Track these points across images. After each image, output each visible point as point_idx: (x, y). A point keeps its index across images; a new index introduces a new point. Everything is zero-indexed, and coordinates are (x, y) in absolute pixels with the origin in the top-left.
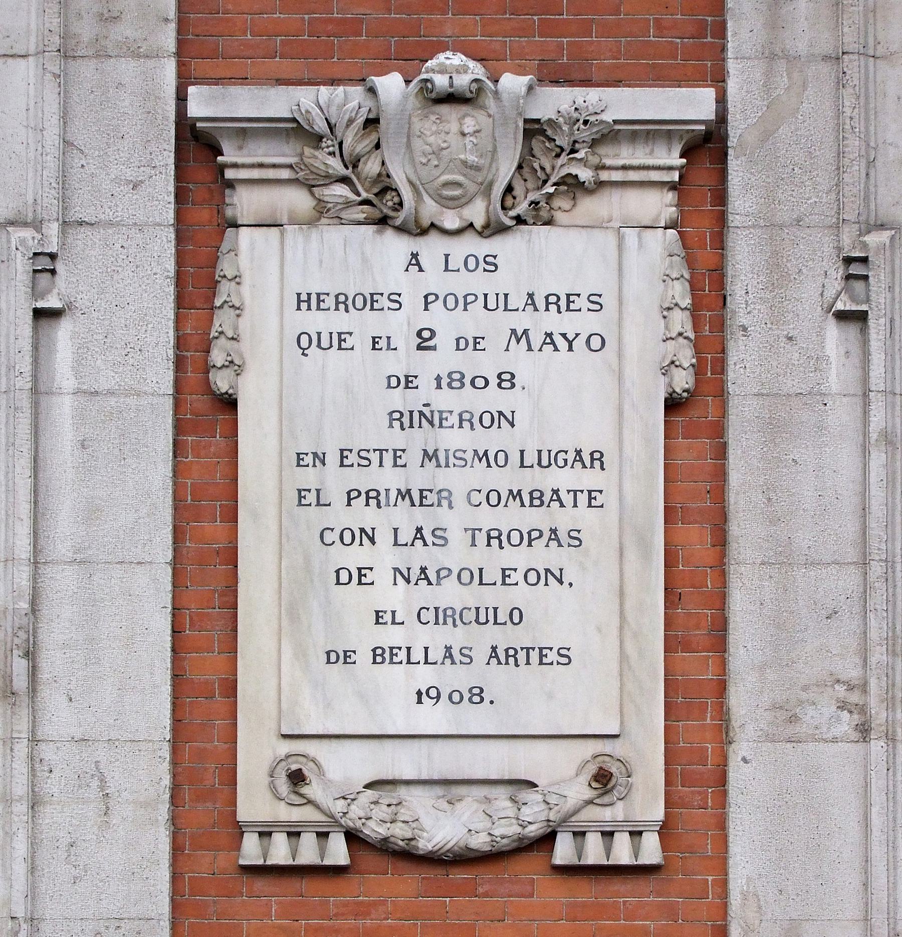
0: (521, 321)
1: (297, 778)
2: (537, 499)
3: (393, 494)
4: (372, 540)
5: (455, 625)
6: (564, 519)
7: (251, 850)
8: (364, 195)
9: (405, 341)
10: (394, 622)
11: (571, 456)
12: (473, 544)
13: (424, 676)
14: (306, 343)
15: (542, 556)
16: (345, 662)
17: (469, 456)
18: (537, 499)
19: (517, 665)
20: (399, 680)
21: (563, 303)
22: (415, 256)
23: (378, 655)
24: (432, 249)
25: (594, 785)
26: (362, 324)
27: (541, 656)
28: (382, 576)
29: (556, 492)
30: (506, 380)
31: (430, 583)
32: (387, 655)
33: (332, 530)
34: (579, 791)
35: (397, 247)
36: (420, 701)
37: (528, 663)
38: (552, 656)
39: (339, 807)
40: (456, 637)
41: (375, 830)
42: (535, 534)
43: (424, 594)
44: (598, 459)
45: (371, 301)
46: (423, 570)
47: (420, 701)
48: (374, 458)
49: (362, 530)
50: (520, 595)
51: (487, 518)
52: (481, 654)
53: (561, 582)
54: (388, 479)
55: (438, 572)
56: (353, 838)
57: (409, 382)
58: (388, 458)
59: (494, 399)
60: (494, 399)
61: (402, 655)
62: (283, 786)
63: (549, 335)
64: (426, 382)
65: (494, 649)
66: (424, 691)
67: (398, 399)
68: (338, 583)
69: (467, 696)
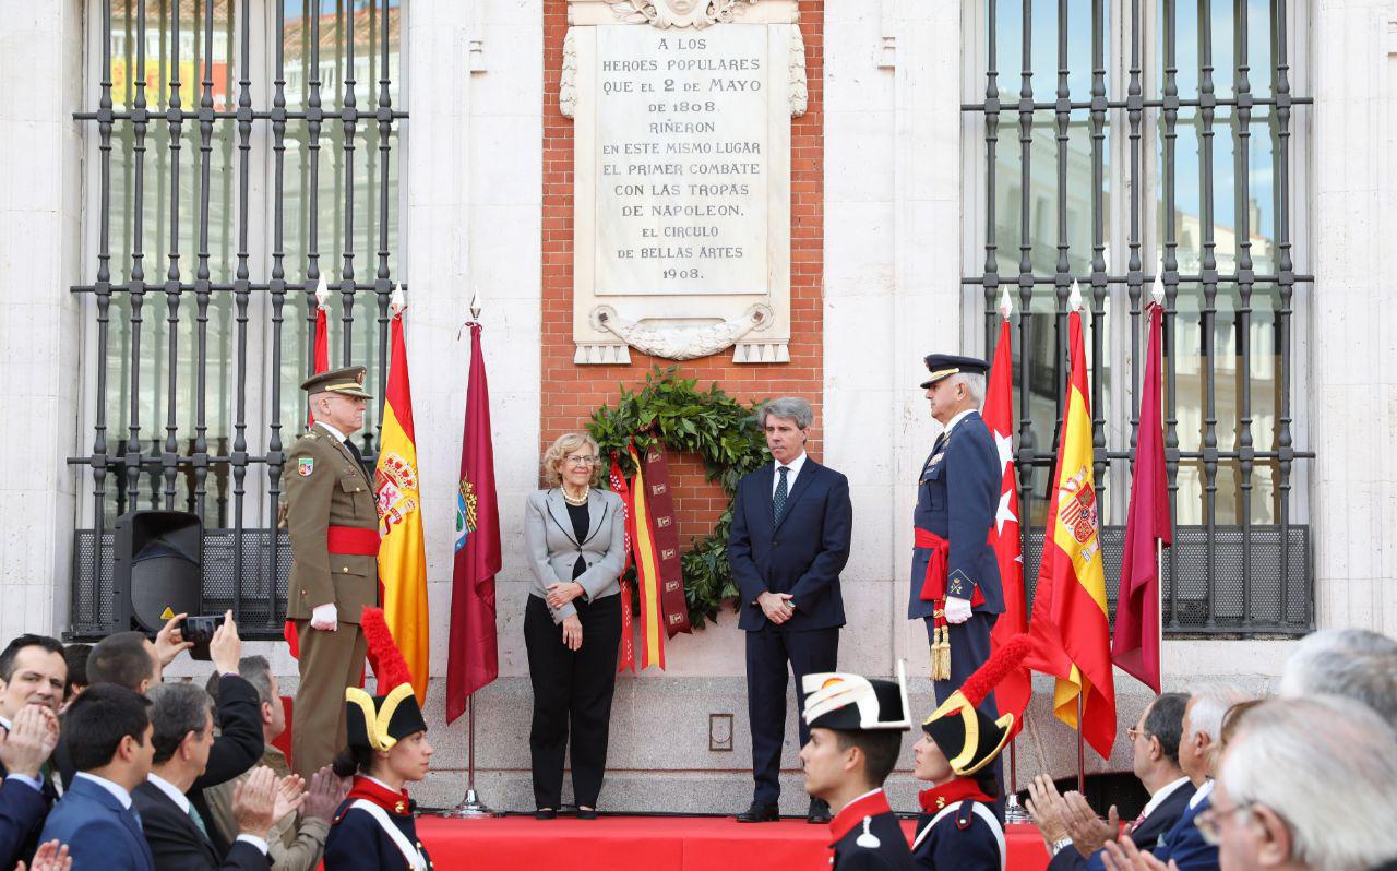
0: (717, 75)
1: (603, 318)
2: (725, 169)
3: (652, 167)
6: (738, 179)
8: (638, 9)
9: (659, 86)
11: (743, 146)
13: (668, 264)
14: (608, 87)
15: (727, 199)
17: (691, 147)
18: (725, 169)
20: (654, 266)
21: (739, 64)
22: (663, 41)
24: (672, 36)
26: (636, 77)
28: (646, 211)
29: (735, 165)
30: (710, 106)
34: (747, 322)
35: (652, 35)
38: (732, 252)
39: (624, 333)
40: (685, 242)
41: (642, 345)
42: (724, 188)
43: (668, 221)
44: (756, 147)
45: (641, 65)
46: (667, 207)
48: (643, 148)
51: (700, 180)
52: (697, 251)
53: (737, 213)
54: (648, 159)
56: (631, 348)
57: (660, 108)
58: (650, 148)
59: (704, 116)
60: (704, 116)
63: (732, 82)
64: (669, 108)
65: (703, 249)
67: (657, 118)
68: (624, 215)
69: (689, 273)
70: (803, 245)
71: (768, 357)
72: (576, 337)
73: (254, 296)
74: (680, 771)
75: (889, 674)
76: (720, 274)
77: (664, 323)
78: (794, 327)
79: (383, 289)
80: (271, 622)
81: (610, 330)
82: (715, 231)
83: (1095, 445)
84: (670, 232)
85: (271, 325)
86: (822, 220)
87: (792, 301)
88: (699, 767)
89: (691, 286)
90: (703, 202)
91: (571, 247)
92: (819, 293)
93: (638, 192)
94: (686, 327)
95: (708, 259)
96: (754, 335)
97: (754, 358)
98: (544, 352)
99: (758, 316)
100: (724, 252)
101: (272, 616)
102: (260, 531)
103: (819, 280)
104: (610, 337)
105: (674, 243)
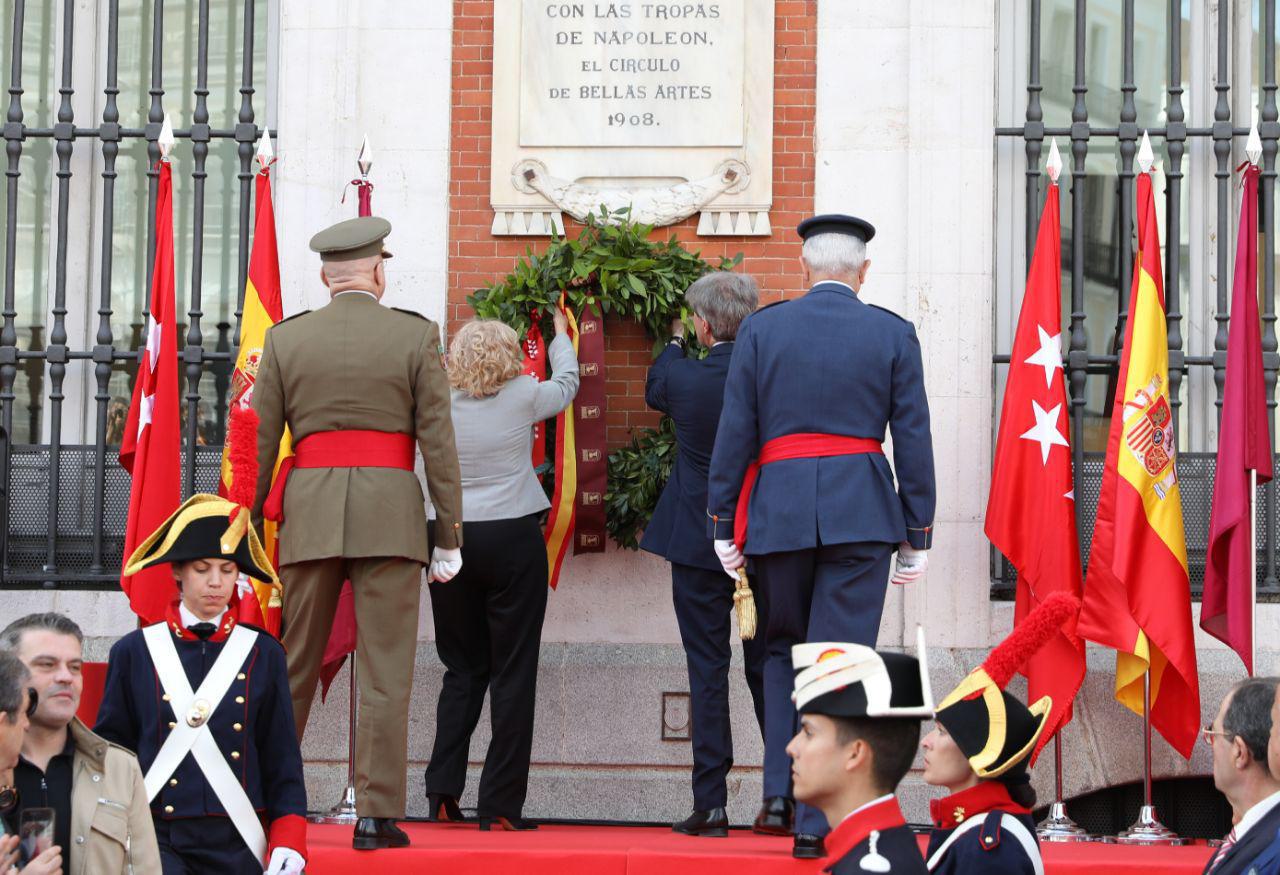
4: (581, 14)
5: (634, 71)
7: (499, 226)
10: (595, 69)
12: (648, 16)
13: (615, 106)
15: (693, 23)
16: (562, 97)
19: (675, 98)
23: (585, 92)
25: (726, 180)
27: (691, 92)
28: (587, 38)
31: (618, 43)
32: (590, 92)
33: (555, 6)
34: (717, 183)
36: (611, 123)
37: (682, 96)
38: (698, 93)
39: (556, 196)
42: (688, 9)
43: (615, 51)
46: (614, 34)
47: (611, 123)
49: (575, 7)
50: (677, 50)
52: (652, 91)
53: (705, 41)
55: (624, 36)
56: (565, 215)
61: (600, 92)
62: (521, 181)
65: (660, 88)
66: (614, 116)
68: (558, 42)
70: (790, 83)
71: (743, 228)
72: (494, 201)
73: (80, 143)
74: (624, 766)
75: (897, 642)
76: (683, 121)
77: (608, 184)
78: (777, 190)
79: (246, 134)
80: (96, 567)
81: (538, 192)
82: (676, 65)
83: (1170, 347)
84: (617, 65)
85: (101, 182)
86: (814, 51)
87: (775, 157)
88: (648, 762)
89: (646, 135)
90: (660, 27)
91: (488, 84)
92: (810, 146)
93: (577, 13)
94: (637, 189)
95: (666, 100)
96: (723, 200)
97: (725, 228)
98: (453, 219)
99: (731, 175)
100: (687, 92)
101: (97, 558)
102: (83, 448)
103: (811, 129)
104: (539, 200)
105: (622, 80)
